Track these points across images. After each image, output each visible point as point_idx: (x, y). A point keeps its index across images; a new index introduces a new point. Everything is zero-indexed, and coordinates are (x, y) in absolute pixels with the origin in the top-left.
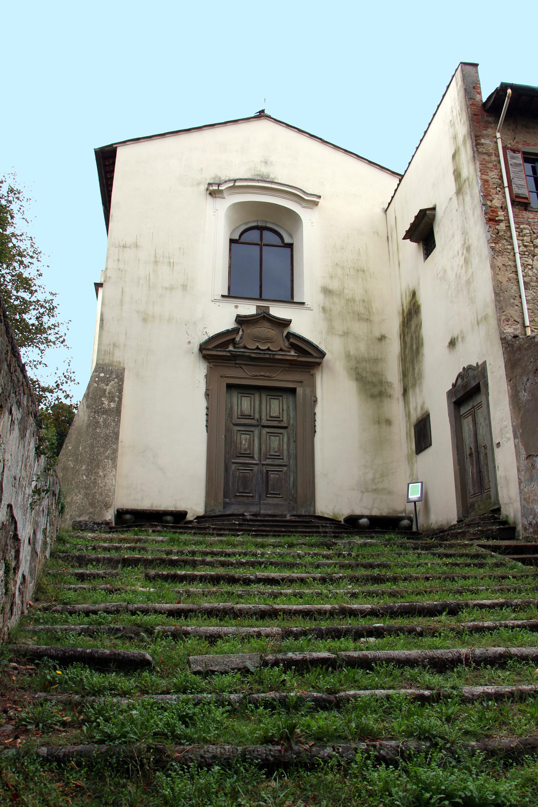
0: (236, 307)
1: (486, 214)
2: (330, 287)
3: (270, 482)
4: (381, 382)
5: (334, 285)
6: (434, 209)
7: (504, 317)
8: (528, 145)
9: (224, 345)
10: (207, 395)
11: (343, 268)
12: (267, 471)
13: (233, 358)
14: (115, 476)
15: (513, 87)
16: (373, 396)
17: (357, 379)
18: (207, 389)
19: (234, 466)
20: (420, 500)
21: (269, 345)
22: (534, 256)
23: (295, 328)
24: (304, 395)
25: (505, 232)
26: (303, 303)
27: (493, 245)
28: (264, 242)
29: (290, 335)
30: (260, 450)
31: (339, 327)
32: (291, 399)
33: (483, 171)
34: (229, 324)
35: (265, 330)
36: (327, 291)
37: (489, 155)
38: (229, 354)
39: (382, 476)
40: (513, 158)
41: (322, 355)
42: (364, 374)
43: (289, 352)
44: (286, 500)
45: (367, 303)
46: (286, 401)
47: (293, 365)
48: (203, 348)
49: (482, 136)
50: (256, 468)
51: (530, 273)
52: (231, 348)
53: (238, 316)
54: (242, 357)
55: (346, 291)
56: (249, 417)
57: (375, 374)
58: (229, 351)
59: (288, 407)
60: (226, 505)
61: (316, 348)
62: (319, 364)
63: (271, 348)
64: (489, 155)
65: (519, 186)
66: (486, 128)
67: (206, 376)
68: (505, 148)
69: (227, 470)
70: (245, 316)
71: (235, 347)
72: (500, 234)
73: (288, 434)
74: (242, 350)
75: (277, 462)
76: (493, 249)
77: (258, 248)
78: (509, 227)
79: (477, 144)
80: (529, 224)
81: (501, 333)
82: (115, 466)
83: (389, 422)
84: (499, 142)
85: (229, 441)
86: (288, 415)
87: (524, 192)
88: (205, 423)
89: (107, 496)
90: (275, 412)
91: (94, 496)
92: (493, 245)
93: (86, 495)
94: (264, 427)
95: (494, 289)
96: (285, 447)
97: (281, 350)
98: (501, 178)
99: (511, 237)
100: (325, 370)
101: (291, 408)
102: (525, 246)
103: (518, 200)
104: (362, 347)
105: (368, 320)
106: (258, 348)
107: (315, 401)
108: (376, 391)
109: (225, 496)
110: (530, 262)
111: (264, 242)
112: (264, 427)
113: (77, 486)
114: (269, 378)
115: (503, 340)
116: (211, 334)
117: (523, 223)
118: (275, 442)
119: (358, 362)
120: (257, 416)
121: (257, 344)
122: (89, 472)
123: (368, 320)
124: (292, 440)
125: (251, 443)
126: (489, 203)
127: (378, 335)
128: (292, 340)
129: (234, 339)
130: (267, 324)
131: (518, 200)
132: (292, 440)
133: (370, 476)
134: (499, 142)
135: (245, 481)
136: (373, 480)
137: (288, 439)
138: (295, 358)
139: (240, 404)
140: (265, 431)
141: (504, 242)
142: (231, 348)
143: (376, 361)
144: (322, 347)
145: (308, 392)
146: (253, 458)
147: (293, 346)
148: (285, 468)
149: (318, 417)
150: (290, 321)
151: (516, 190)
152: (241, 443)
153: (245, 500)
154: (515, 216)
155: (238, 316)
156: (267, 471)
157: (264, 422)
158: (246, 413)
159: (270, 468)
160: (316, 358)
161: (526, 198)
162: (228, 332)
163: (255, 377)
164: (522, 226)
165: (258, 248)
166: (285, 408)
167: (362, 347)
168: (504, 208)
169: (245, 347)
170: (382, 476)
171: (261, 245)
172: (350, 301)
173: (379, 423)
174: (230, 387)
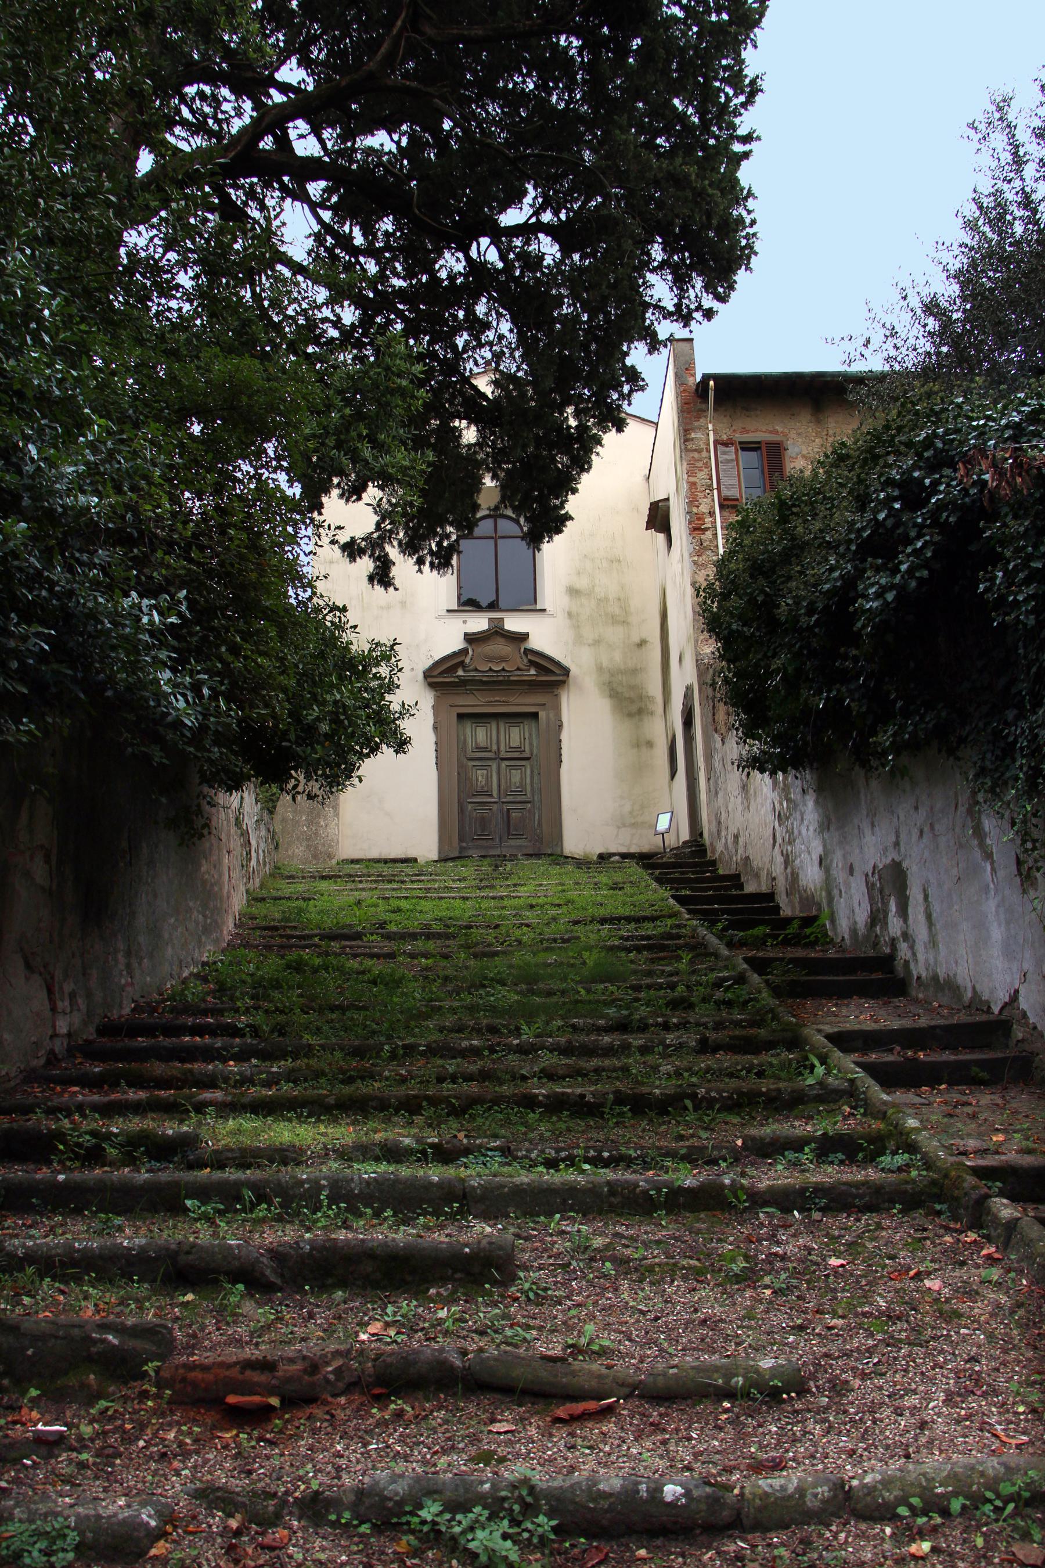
0: (465, 622)
1: (690, 523)
2: (578, 586)
4: (641, 698)
5: (582, 583)
6: (668, 499)
8: (748, 432)
9: (453, 669)
10: (435, 728)
11: (593, 560)
13: (463, 683)
14: (337, 825)
15: (716, 377)
16: (630, 715)
17: (611, 696)
19: (470, 806)
20: (668, 831)
28: (499, 534)
29: (528, 651)
30: (499, 786)
31: (589, 633)
32: (533, 725)
33: (690, 473)
34: (457, 644)
35: (499, 647)
36: (573, 592)
37: (699, 451)
39: (643, 807)
40: (724, 453)
41: (566, 671)
42: (620, 689)
45: (623, 602)
46: (527, 726)
47: (533, 686)
48: (428, 674)
49: (693, 429)
50: (495, 807)
52: (460, 673)
53: (466, 634)
54: (472, 681)
55: (597, 589)
56: (484, 749)
57: (632, 688)
60: (462, 849)
61: (557, 664)
62: (564, 682)
64: (699, 451)
65: (730, 487)
66: (698, 418)
67: (434, 707)
68: (716, 442)
69: (462, 810)
70: (474, 634)
75: (519, 799)
76: (695, 563)
77: (492, 542)
79: (686, 440)
81: (698, 654)
82: (337, 815)
83: (650, 744)
84: (711, 434)
85: (463, 778)
86: (531, 744)
87: (734, 493)
89: (330, 846)
90: (515, 741)
91: (316, 848)
93: (308, 846)
96: (528, 780)
97: (518, 669)
98: (711, 479)
99: (717, 547)
100: (572, 688)
104: (618, 657)
105: (625, 623)
106: (491, 670)
107: (561, 726)
108: (634, 708)
109: (461, 839)
111: (499, 534)
113: (298, 838)
114: (505, 703)
116: (437, 658)
118: (516, 776)
119: (612, 675)
120: (495, 748)
122: (310, 823)
123: (625, 623)
126: (695, 510)
127: (636, 639)
130: (501, 640)
133: (627, 808)
134: (711, 434)
136: (631, 813)
137: (532, 772)
139: (474, 736)
140: (504, 764)
141: (709, 553)
142: (460, 673)
143: (635, 671)
144: (565, 662)
145: (551, 715)
146: (491, 796)
147: (532, 663)
149: (565, 745)
150: (527, 634)
151: (725, 492)
153: (484, 843)
155: (466, 634)
157: (503, 755)
158: (482, 745)
162: (454, 655)
163: (489, 703)
165: (492, 542)
167: (618, 657)
168: (712, 514)
169: (476, 670)
170: (643, 807)
171: (495, 538)
172: (602, 601)
173: (638, 745)
174: (461, 717)
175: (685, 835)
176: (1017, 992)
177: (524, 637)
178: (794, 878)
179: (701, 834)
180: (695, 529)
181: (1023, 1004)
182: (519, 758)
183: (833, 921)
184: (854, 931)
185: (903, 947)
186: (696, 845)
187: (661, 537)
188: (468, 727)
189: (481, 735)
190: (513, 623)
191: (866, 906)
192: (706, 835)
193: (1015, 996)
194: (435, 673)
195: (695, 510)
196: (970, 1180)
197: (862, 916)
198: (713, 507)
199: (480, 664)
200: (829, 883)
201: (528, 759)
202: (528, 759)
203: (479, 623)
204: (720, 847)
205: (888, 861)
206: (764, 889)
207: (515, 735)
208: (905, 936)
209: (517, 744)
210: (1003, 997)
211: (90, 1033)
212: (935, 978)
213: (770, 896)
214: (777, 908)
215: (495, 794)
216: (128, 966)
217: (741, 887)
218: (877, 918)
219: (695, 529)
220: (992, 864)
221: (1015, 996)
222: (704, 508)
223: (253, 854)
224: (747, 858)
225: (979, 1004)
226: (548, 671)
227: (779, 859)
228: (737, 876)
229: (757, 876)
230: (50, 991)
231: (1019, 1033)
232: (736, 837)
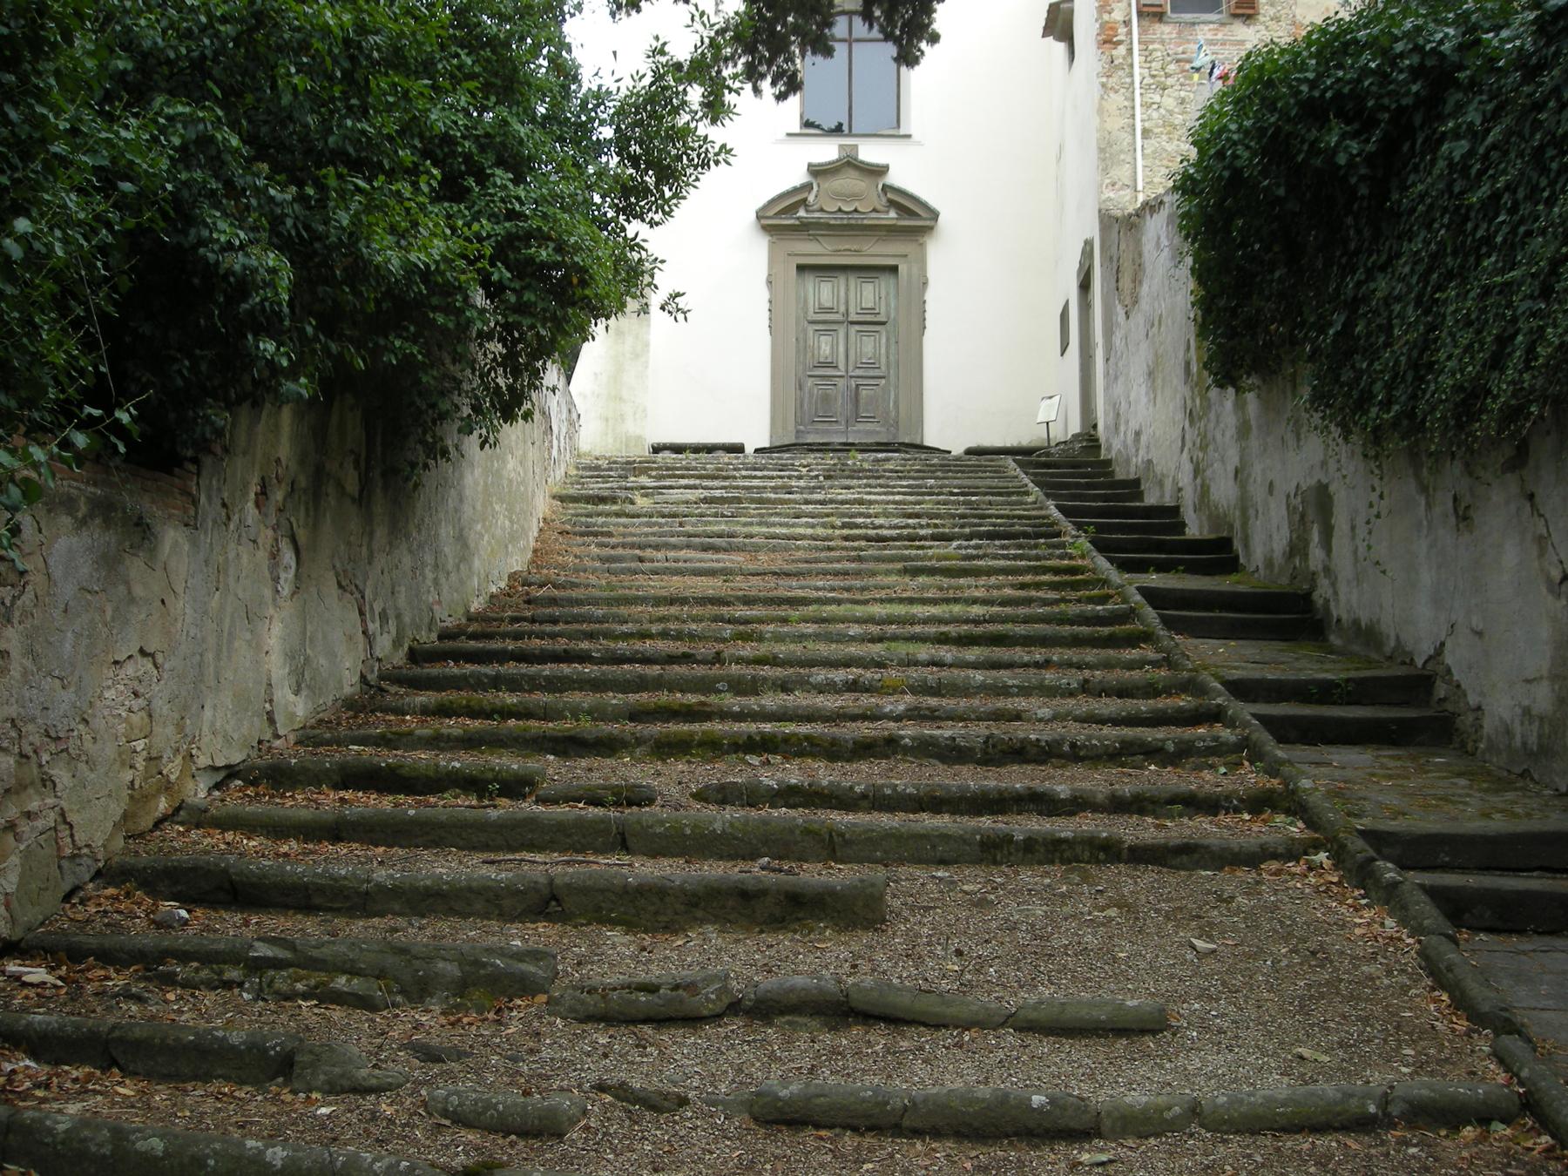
3: (862, 402)
7: (1108, 181)
9: (792, 209)
10: (769, 283)
12: (857, 386)
18: (769, 275)
19: (810, 382)
21: (857, 204)
22: (1164, 89)
23: (895, 178)
24: (910, 275)
25: (1124, 58)
26: (909, 136)
27: (1104, 80)
29: (886, 188)
32: (892, 280)
34: (799, 177)
35: (849, 182)
38: (797, 223)
41: (935, 215)
43: (887, 212)
44: (883, 426)
46: (885, 282)
47: (892, 231)
48: (760, 215)
50: (841, 383)
51: (1155, 115)
53: (810, 165)
54: (818, 225)
56: (830, 310)
58: (798, 218)
59: (888, 294)
61: (925, 206)
62: (931, 228)
63: (860, 209)
71: (807, 211)
72: (1116, 62)
73: (887, 332)
74: (817, 215)
75: (871, 373)
76: (1103, 85)
78: (1130, 51)
80: (1162, 42)
85: (802, 347)
86: (888, 305)
88: (767, 323)
92: (1104, 80)
94: (853, 323)
95: (1098, 143)
96: (883, 351)
97: (875, 210)
101: (892, 296)
102: (1153, 76)
103: (1146, 9)
106: (840, 210)
107: (925, 284)
110: (1157, 98)
111: (854, 35)
112: (853, 323)
115: (1100, 211)
117: (1153, 42)
120: (842, 309)
121: (840, 204)
124: (893, 340)
125: (834, 348)
128: (889, 195)
129: (805, 200)
130: (853, 173)
131: (1146, 9)
132: (893, 340)
135: (826, 399)
137: (888, 339)
138: (894, 222)
142: (802, 213)
144: (933, 202)
145: (915, 270)
147: (892, 204)
148: (883, 381)
152: (819, 348)
153: (826, 426)
154: (1142, 32)
155: (810, 165)
156: (857, 386)
157: (853, 317)
158: (828, 305)
159: (860, 381)
160: (925, 219)
161: (1160, 6)
162: (795, 191)
164: (1151, 47)
166: (883, 295)
168: (1127, 23)
169: (822, 210)
174: (801, 268)
175: (1075, 427)
176: (1443, 644)
177: (879, 171)
178: (1204, 492)
179: (1095, 427)
180: (1105, 42)
181: (1449, 659)
182: (871, 323)
183: (1246, 546)
184: (1269, 563)
185: (1323, 583)
186: (1089, 439)
187: (1060, 48)
188: (810, 281)
189: (825, 292)
190: (869, 152)
191: (1285, 532)
192: (1101, 427)
193: (1440, 649)
194: (771, 213)
195: (1106, 17)
196: (1360, 843)
197: (1280, 542)
198: (1129, 14)
199: (824, 201)
200: (1244, 504)
201: (883, 323)
202: (883, 323)
203: (827, 151)
204: (1117, 444)
205: (1312, 482)
206: (1168, 501)
207: (868, 294)
208: (1327, 570)
209: (870, 305)
210: (1425, 649)
211: (399, 658)
212: (1356, 622)
213: (1174, 511)
214: (1184, 525)
215: (842, 366)
216: (436, 582)
217: (1139, 496)
218: (1297, 548)
219: (1105, 42)
220: (1427, 498)
221: (1440, 649)
222: (1118, 16)
223: (555, 442)
224: (1150, 462)
225: (1402, 655)
226: (911, 214)
227: (1188, 468)
228: (1136, 483)
229: (1161, 484)
230: (361, 613)
231: (1441, 690)
232: (1138, 434)
